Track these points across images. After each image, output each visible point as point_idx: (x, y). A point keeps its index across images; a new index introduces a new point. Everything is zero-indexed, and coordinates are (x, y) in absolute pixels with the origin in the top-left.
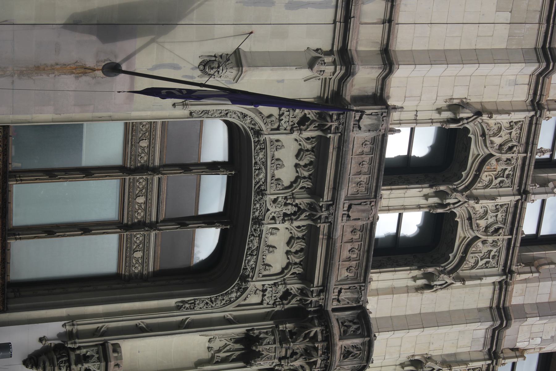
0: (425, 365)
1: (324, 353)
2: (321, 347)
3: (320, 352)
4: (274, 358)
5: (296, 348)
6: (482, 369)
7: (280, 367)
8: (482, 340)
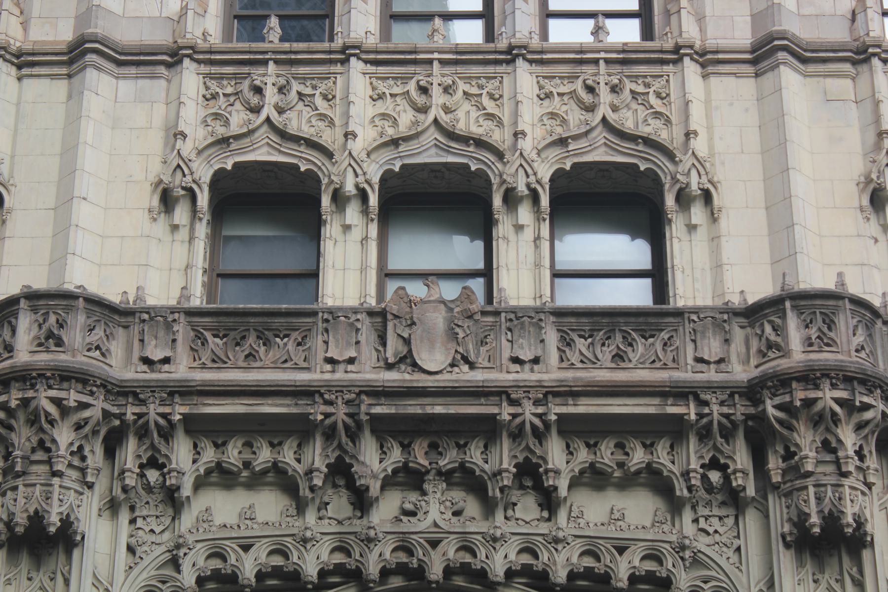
0: (167, 184)
1: (33, 386)
2: (21, 393)
3: (30, 394)
4: (51, 485)
5: (27, 444)
6: (207, 74)
7: (87, 473)
8: (141, 82)
